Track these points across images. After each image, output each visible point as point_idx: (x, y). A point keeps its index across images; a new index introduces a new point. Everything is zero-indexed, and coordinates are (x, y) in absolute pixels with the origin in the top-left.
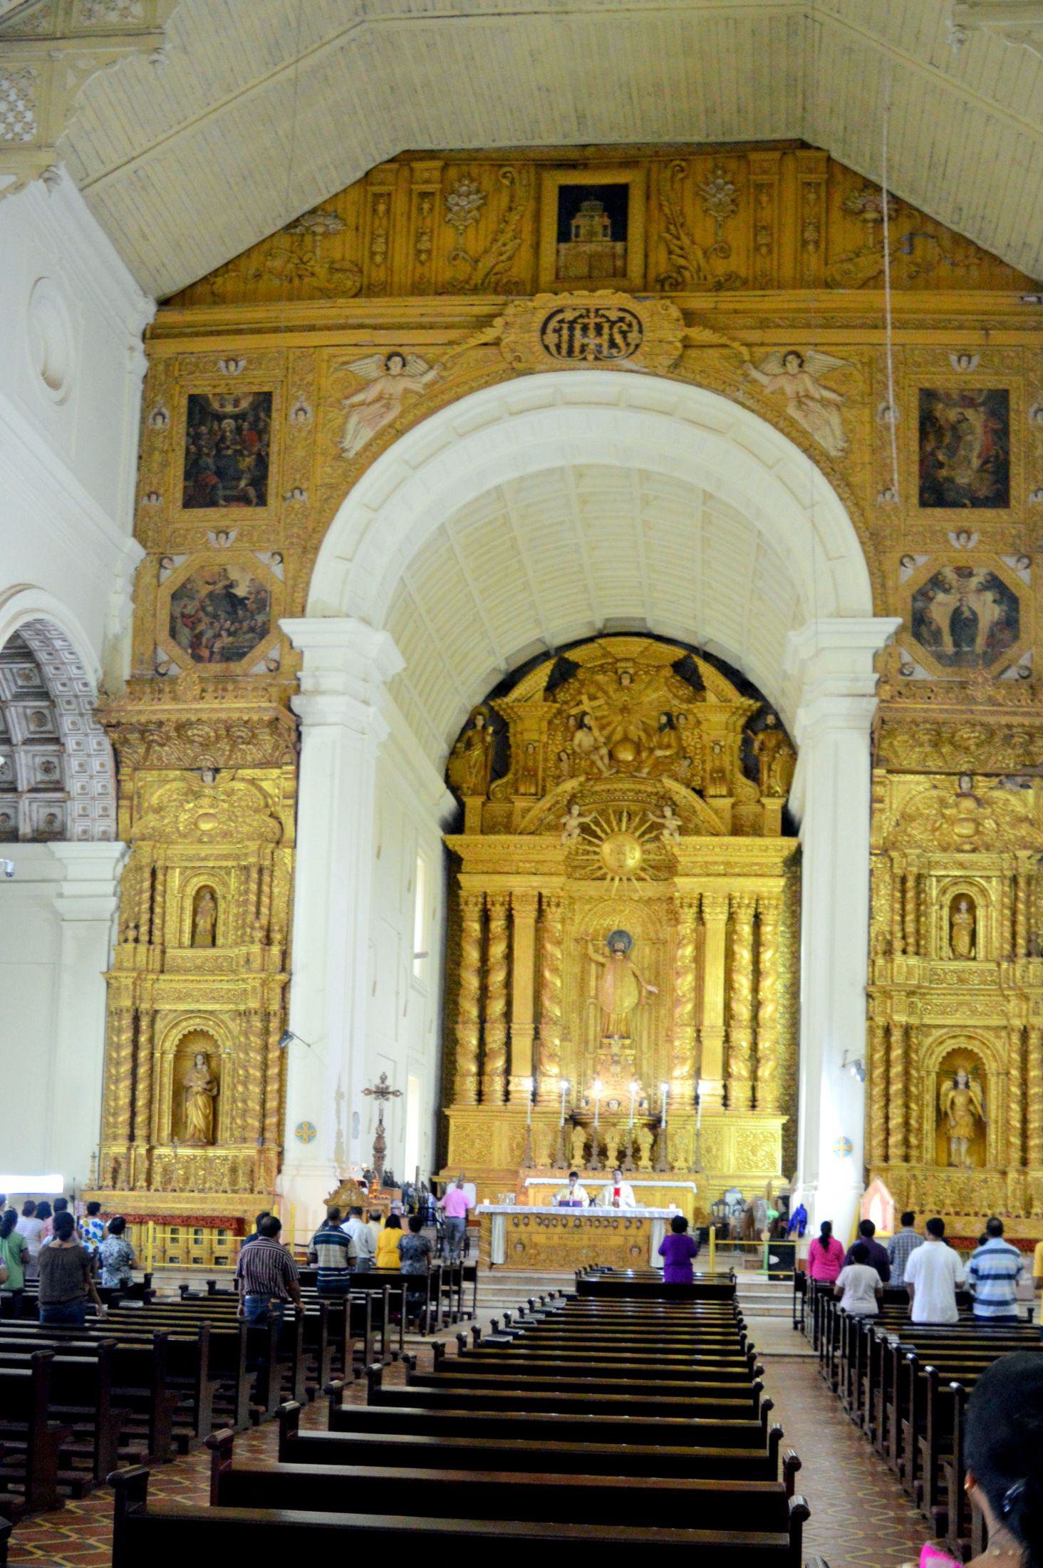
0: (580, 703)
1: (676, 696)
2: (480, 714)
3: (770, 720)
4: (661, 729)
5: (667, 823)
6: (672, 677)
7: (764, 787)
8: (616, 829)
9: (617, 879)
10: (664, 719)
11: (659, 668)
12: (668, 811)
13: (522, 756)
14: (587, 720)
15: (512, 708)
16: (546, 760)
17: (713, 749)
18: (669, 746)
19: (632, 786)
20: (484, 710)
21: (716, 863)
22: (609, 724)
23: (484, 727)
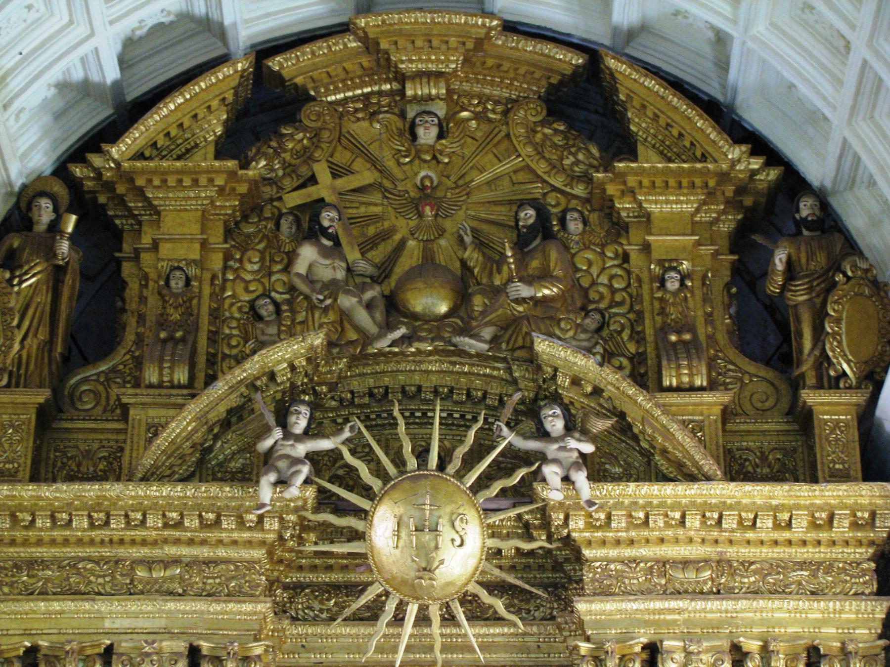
0: (312, 180)
1: (556, 167)
2: (43, 194)
3: (806, 208)
4: (522, 243)
5: (552, 449)
6: (543, 123)
7: (807, 367)
8: (412, 463)
9: (412, 610)
10: (528, 215)
11: (509, 106)
12: (555, 424)
13: (153, 301)
14: (327, 218)
15: (129, 178)
16: (215, 315)
17: (662, 282)
18: (543, 276)
19: (449, 380)
20: (59, 188)
21: (685, 564)
22: (384, 236)
23: (55, 227)
